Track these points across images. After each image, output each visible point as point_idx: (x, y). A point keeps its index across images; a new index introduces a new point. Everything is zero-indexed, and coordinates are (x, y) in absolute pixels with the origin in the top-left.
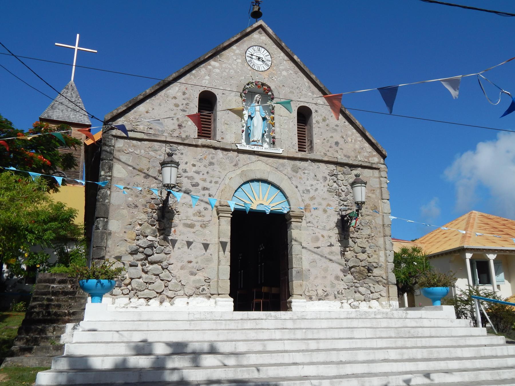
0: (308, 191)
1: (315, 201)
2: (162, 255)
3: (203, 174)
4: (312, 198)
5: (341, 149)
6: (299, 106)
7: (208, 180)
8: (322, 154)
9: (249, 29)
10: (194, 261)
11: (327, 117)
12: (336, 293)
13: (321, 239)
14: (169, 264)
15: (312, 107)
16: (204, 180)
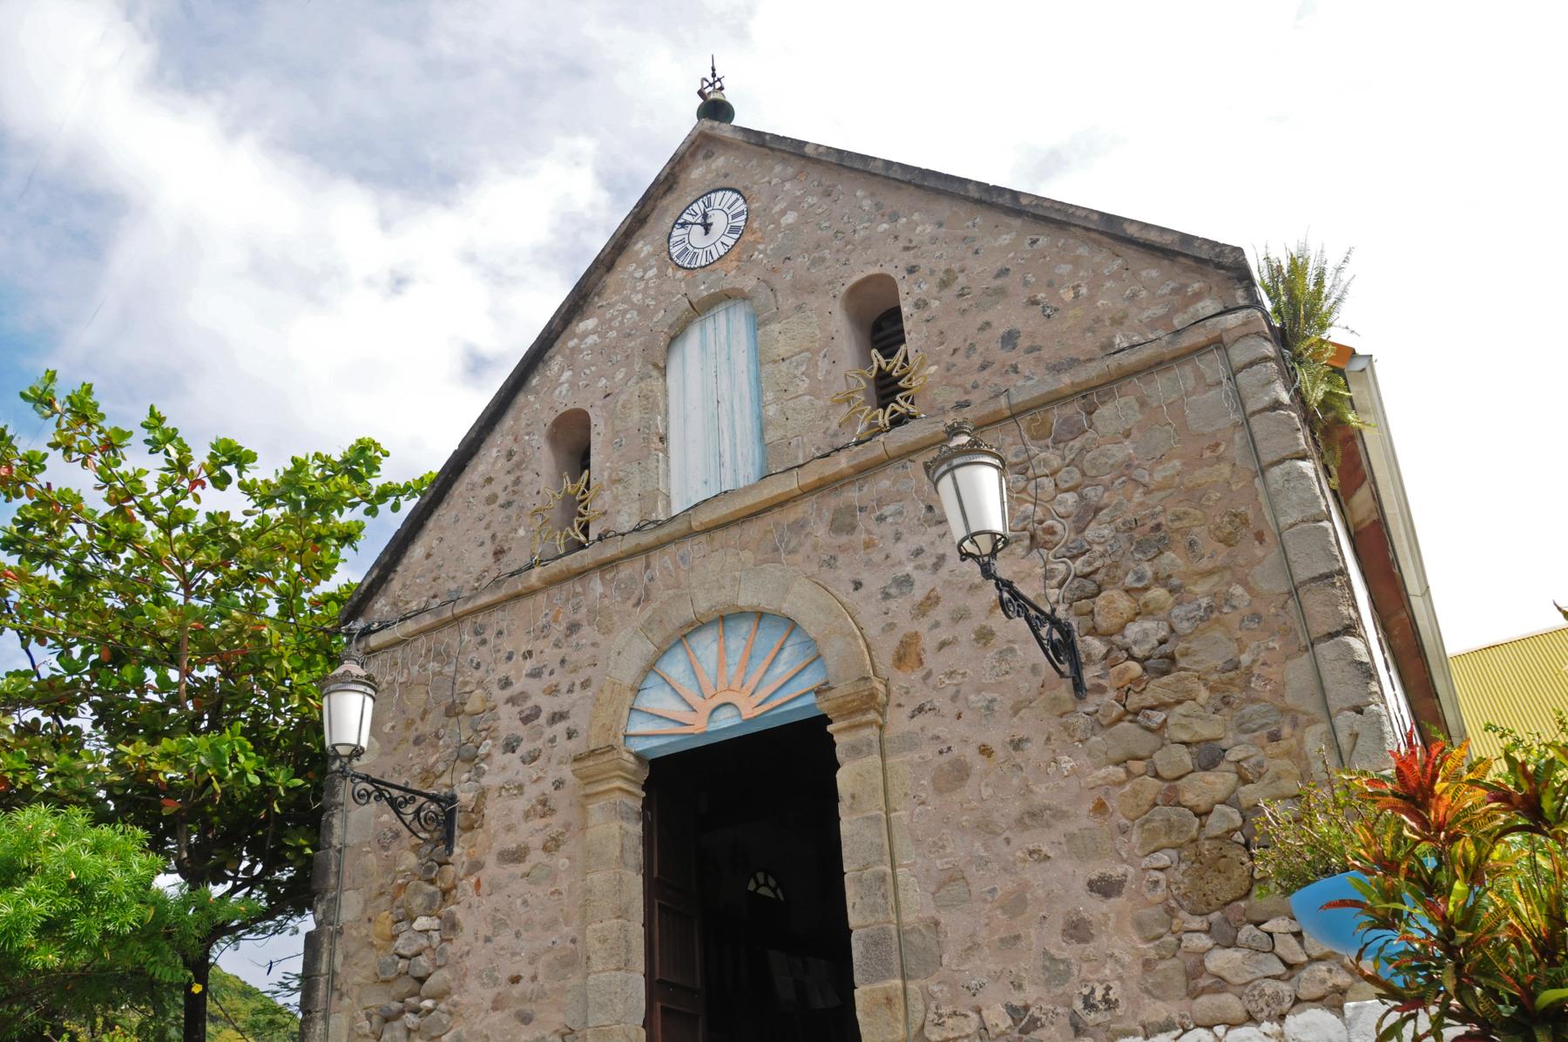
0: (905, 582)
1: (940, 613)
10: (526, 973)
12: (1078, 1005)
13: (978, 764)
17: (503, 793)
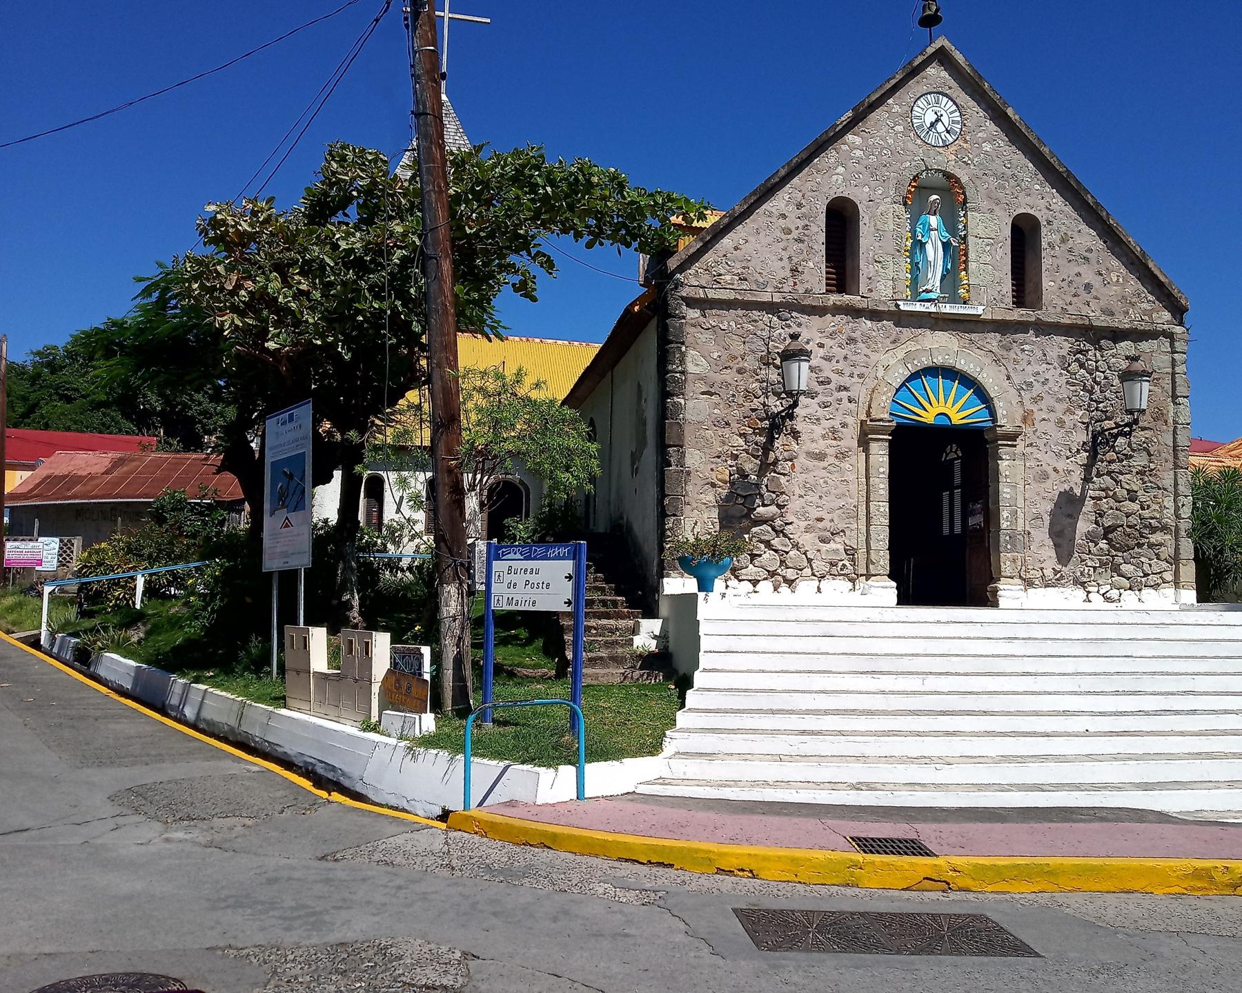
0: (1030, 385)
1: (1043, 405)
2: (773, 509)
4: (1037, 399)
6: (1015, 213)
7: (847, 372)
8: (1059, 309)
10: (827, 517)
11: (1069, 233)
14: (786, 524)
15: (1042, 216)
16: (840, 373)
17: (807, 419)
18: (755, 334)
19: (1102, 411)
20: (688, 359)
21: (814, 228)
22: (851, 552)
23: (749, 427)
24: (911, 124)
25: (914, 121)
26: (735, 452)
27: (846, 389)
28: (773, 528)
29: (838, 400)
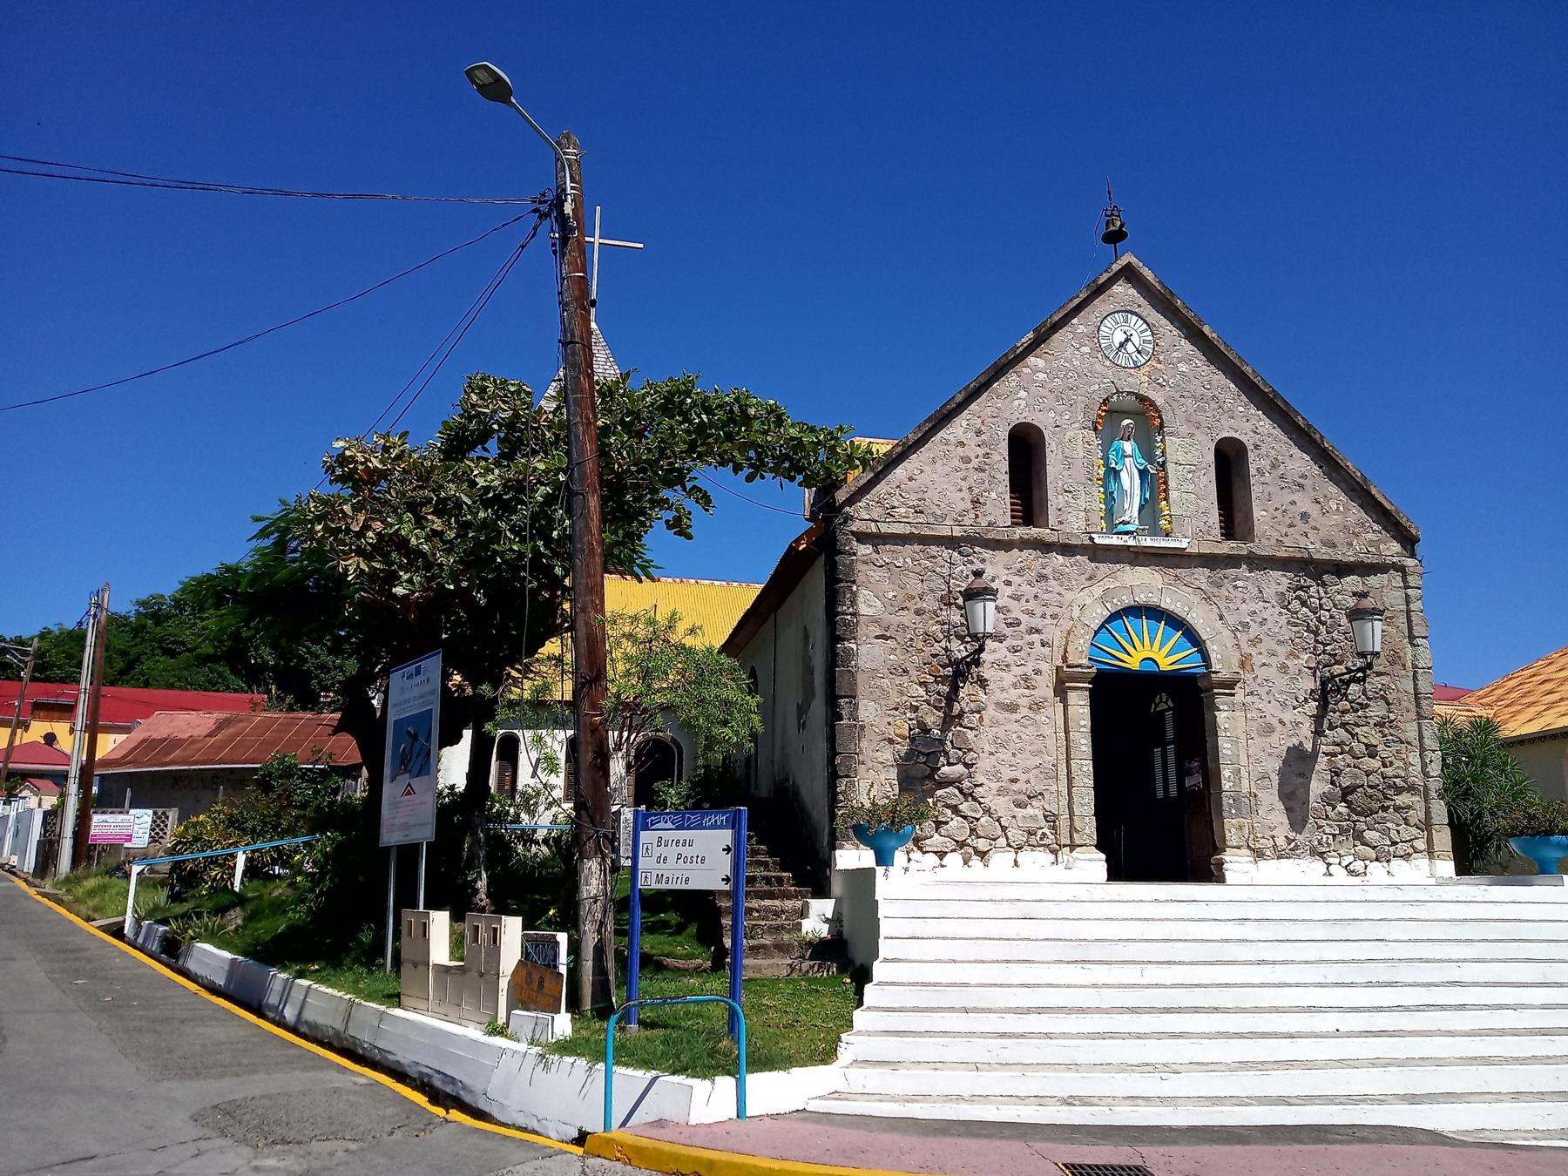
0: (1246, 625)
1: (1262, 647)
3: (1027, 601)
4: (1256, 641)
5: (1315, 528)
7: (1038, 611)
8: (1273, 541)
9: (1105, 277)
10: (1023, 777)
13: (1279, 727)
14: (976, 786)
15: (1248, 440)
16: (1031, 613)
18: (934, 571)
19: (1330, 654)
20: (860, 599)
21: (996, 457)
22: (1051, 818)
23: (930, 675)
24: (1098, 345)
25: (1102, 341)
26: (915, 704)
27: (1038, 631)
28: (961, 791)
29: (1029, 644)
